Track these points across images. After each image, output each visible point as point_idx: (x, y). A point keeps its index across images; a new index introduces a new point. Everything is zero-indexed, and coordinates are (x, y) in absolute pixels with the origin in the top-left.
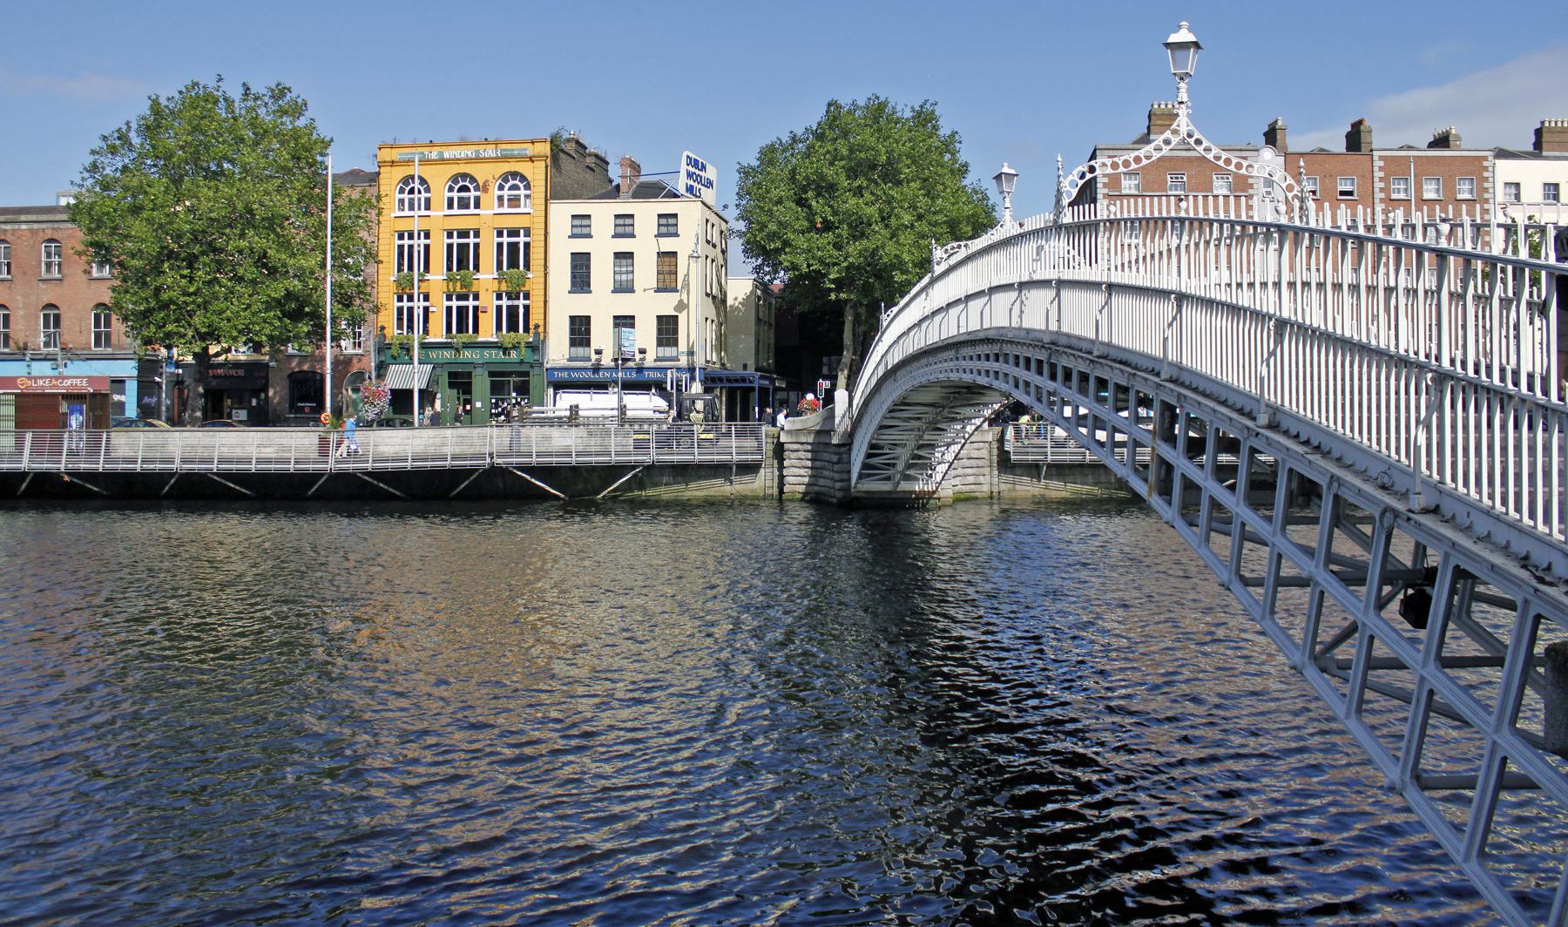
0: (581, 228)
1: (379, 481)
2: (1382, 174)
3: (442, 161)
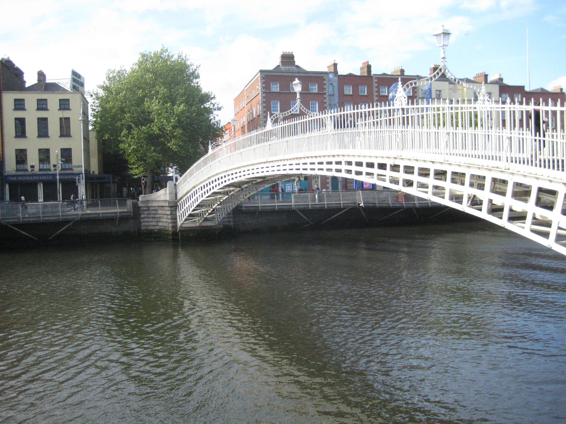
2: (376, 85)
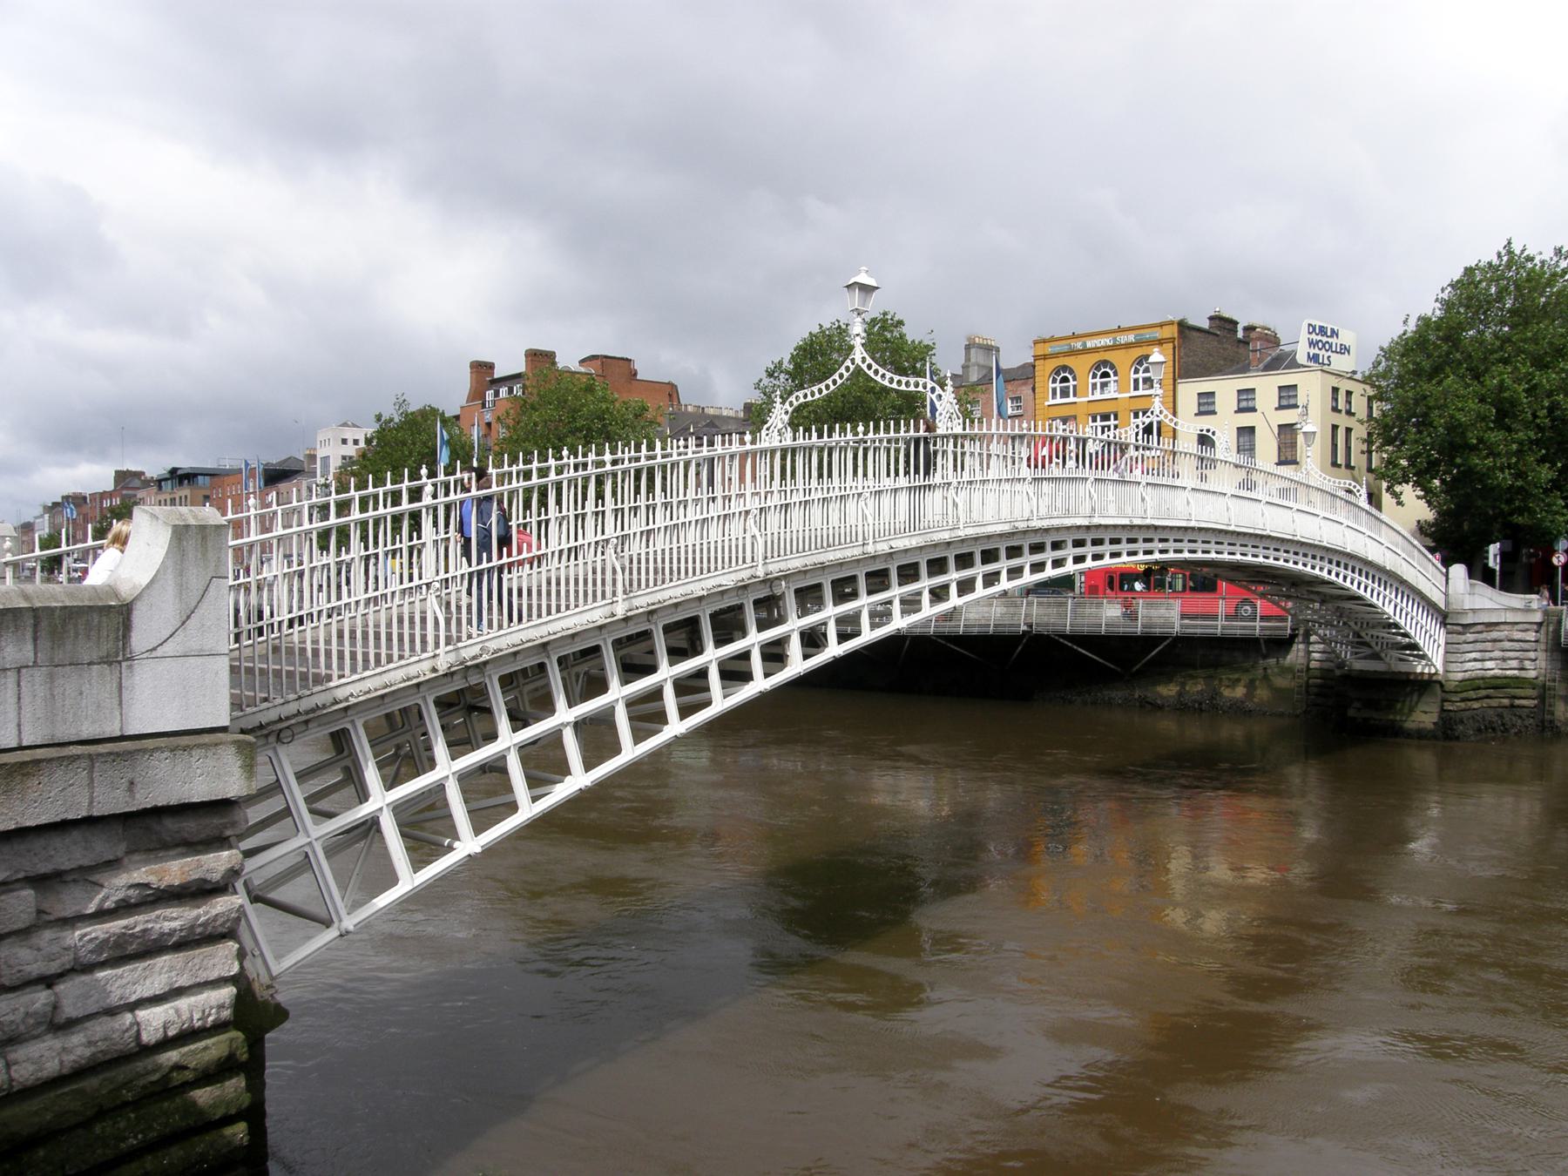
0: (1206, 404)
1: (950, 642)
3: (1086, 351)
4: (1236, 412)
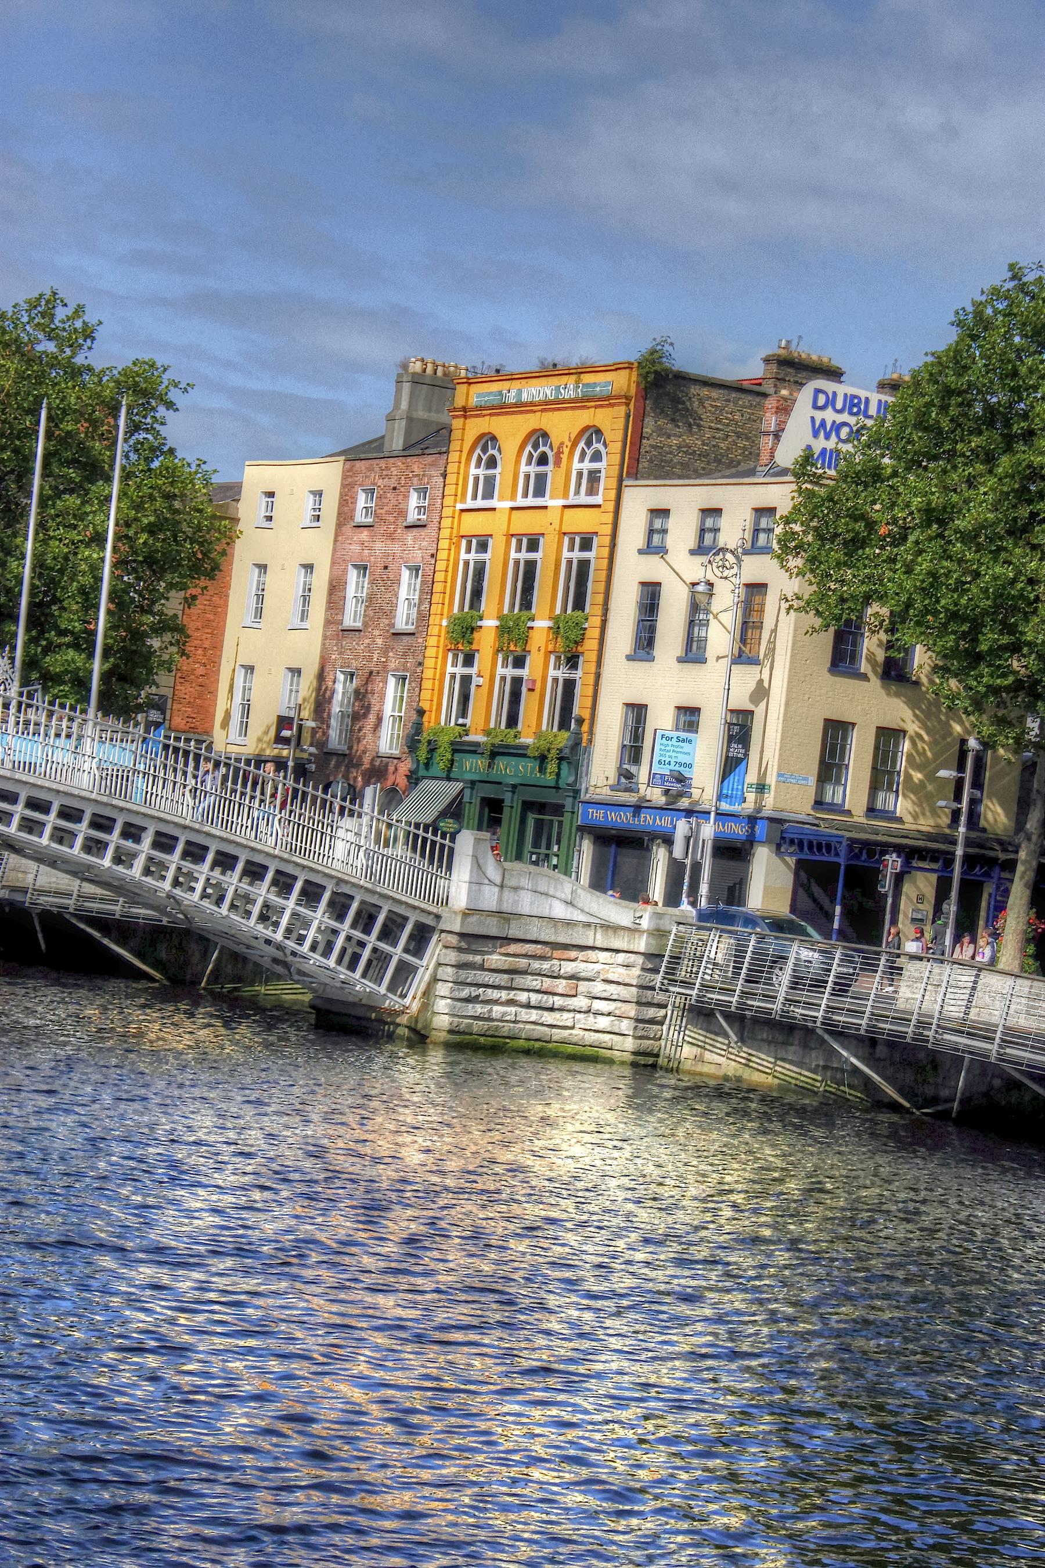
3: (521, 407)
4: (641, 552)
